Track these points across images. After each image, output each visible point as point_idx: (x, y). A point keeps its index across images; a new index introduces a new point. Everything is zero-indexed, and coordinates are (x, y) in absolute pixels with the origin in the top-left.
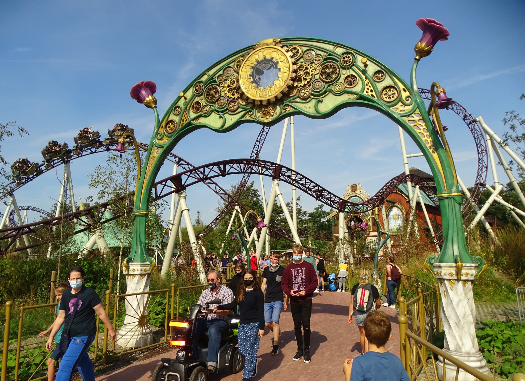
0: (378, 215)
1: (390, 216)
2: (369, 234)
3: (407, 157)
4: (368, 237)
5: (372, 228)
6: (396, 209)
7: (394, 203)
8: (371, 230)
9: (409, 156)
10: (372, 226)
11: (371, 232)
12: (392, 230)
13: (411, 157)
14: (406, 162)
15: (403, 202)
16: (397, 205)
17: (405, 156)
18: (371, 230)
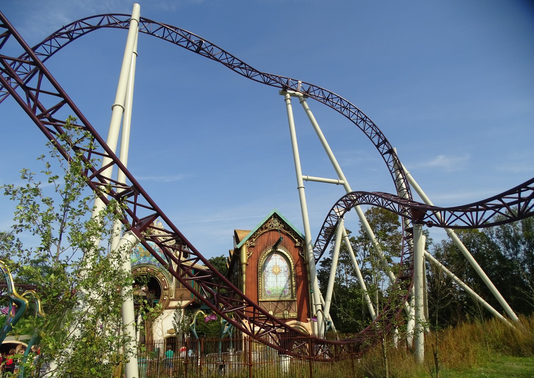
0: (247, 265)
1: (267, 269)
2: (168, 304)
3: (304, 179)
4: (166, 309)
5: (175, 293)
6: (278, 256)
7: (275, 247)
8: (173, 297)
9: (306, 177)
10: (176, 290)
11: (173, 300)
12: (269, 292)
13: (307, 180)
14: (302, 184)
15: (288, 247)
16: (281, 250)
17: (301, 177)
18: (173, 297)
